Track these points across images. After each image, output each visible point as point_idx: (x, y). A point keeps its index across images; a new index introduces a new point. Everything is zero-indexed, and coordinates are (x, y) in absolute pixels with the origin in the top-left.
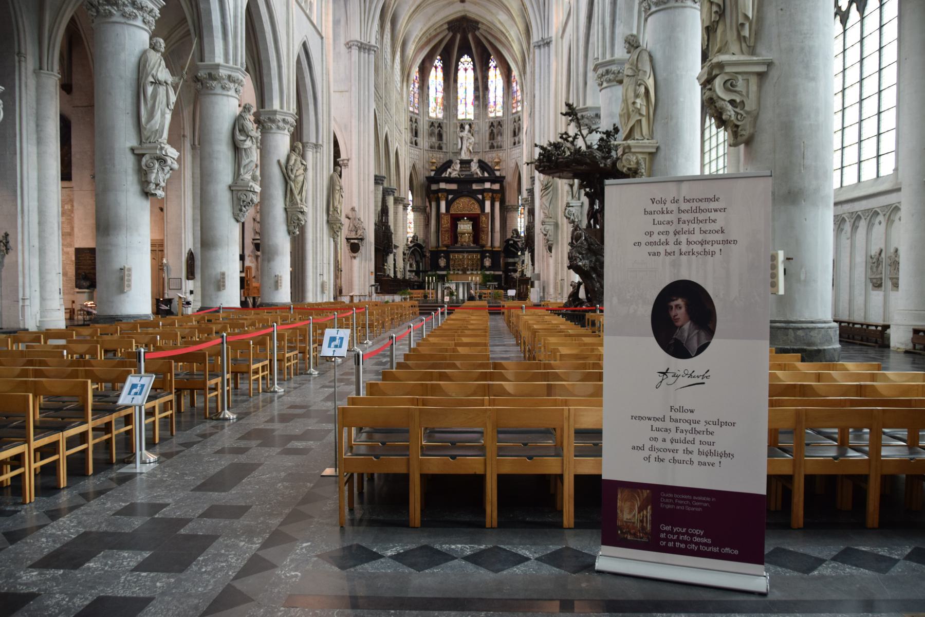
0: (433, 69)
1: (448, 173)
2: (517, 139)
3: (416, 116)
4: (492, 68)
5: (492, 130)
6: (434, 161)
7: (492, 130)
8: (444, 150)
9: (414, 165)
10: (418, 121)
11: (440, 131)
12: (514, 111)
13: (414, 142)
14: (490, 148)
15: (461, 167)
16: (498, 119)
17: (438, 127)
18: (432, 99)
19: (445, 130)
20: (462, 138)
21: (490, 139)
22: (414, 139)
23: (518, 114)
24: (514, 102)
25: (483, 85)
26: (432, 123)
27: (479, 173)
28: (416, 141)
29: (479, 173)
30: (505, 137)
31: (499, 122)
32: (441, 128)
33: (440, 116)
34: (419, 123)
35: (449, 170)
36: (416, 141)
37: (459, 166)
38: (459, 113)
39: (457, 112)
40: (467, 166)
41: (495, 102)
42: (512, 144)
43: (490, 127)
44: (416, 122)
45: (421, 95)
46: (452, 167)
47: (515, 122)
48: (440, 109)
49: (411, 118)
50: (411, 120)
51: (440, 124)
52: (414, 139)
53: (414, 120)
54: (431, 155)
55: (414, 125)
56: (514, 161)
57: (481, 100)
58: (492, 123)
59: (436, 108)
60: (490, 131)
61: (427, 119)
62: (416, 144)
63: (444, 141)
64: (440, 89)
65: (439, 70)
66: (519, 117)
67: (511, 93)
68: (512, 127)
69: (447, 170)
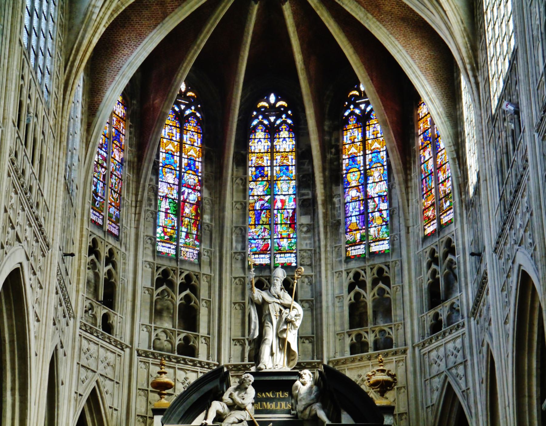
0: (170, 120)
1: (212, 414)
2: (443, 311)
3: (111, 240)
4: (352, 121)
5: (357, 296)
6: (164, 379)
7: (357, 296)
8: (202, 357)
9: (94, 391)
10: (118, 258)
11: (187, 297)
12: (430, 229)
13: (99, 321)
14: (354, 349)
15: (257, 400)
16: (378, 262)
17: (183, 288)
18: (164, 205)
19: (204, 293)
20: (262, 307)
21: (352, 326)
22: (101, 311)
23: (446, 234)
24: (430, 202)
25: (324, 170)
26: (165, 273)
27: (322, 414)
28: (106, 317)
29: (322, 414)
30: (397, 312)
31: (380, 271)
32: (195, 290)
33: (189, 254)
34: (120, 266)
35: (216, 406)
36: (106, 317)
37: (251, 392)
38: (252, 247)
39: (244, 248)
40: (280, 394)
41: (364, 215)
42: (427, 330)
43: (351, 287)
44: (110, 260)
45: (132, 186)
46: (226, 397)
47: (434, 260)
48: (187, 236)
49: (94, 241)
50: (93, 250)
51: (188, 278)
52: (101, 311)
53: (104, 253)
54: (155, 370)
55: (103, 270)
56: (437, 382)
57: (321, 210)
58: (357, 275)
59: (178, 231)
60: (348, 298)
61: (150, 259)
62: (108, 327)
63: (203, 330)
64: (190, 178)
65: (191, 126)
66: (449, 241)
67: (415, 181)
68: (426, 276)
69: (207, 407)
